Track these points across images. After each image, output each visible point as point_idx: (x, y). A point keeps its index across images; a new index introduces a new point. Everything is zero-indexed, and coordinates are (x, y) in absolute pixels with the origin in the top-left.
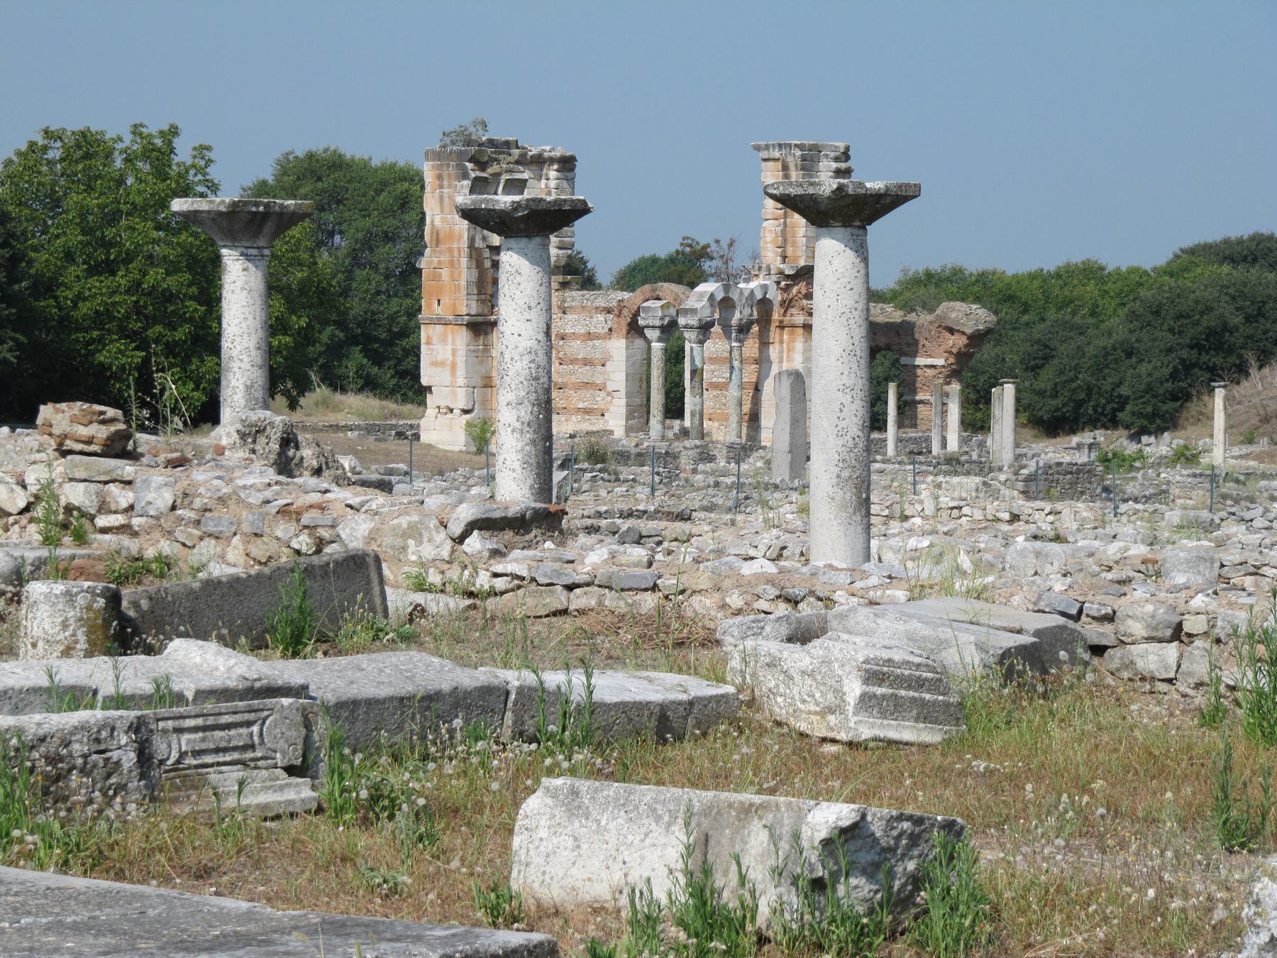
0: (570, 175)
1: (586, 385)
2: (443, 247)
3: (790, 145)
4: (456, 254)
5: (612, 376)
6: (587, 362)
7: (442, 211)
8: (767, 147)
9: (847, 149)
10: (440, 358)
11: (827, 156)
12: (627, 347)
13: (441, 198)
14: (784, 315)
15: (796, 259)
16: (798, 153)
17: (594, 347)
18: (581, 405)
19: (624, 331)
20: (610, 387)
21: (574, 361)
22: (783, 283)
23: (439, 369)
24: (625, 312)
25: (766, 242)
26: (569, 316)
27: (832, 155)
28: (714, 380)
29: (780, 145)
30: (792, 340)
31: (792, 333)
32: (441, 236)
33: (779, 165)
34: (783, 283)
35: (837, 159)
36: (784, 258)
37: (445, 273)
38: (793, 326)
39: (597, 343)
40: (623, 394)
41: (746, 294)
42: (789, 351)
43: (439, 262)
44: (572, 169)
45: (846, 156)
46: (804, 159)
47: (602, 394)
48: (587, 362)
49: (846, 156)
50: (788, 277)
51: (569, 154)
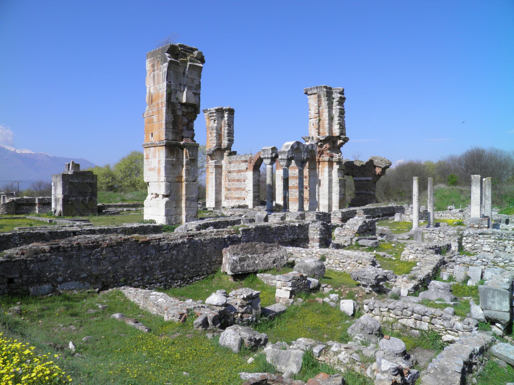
0: (232, 116)
1: (238, 189)
2: (154, 103)
3: (321, 87)
4: (160, 106)
6: (238, 180)
7: (154, 84)
8: (311, 89)
9: (343, 90)
10: (152, 166)
11: (336, 92)
12: (253, 175)
13: (154, 76)
14: (320, 157)
15: (324, 133)
16: (325, 90)
18: (236, 196)
19: (252, 169)
20: (247, 189)
21: (234, 180)
22: (319, 144)
23: (152, 172)
24: (252, 161)
25: (311, 128)
26: (232, 165)
27: (338, 91)
29: (317, 88)
30: (323, 167)
31: (323, 164)
32: (154, 97)
33: (317, 95)
34: (319, 144)
35: (340, 93)
36: (319, 133)
37: (155, 118)
38: (324, 161)
39: (242, 173)
41: (306, 147)
42: (322, 172)
43: (152, 113)
44: (233, 114)
45: (342, 93)
46: (327, 92)
47: (244, 192)
48: (238, 180)
49: (342, 93)
50: (321, 141)
51: (232, 108)
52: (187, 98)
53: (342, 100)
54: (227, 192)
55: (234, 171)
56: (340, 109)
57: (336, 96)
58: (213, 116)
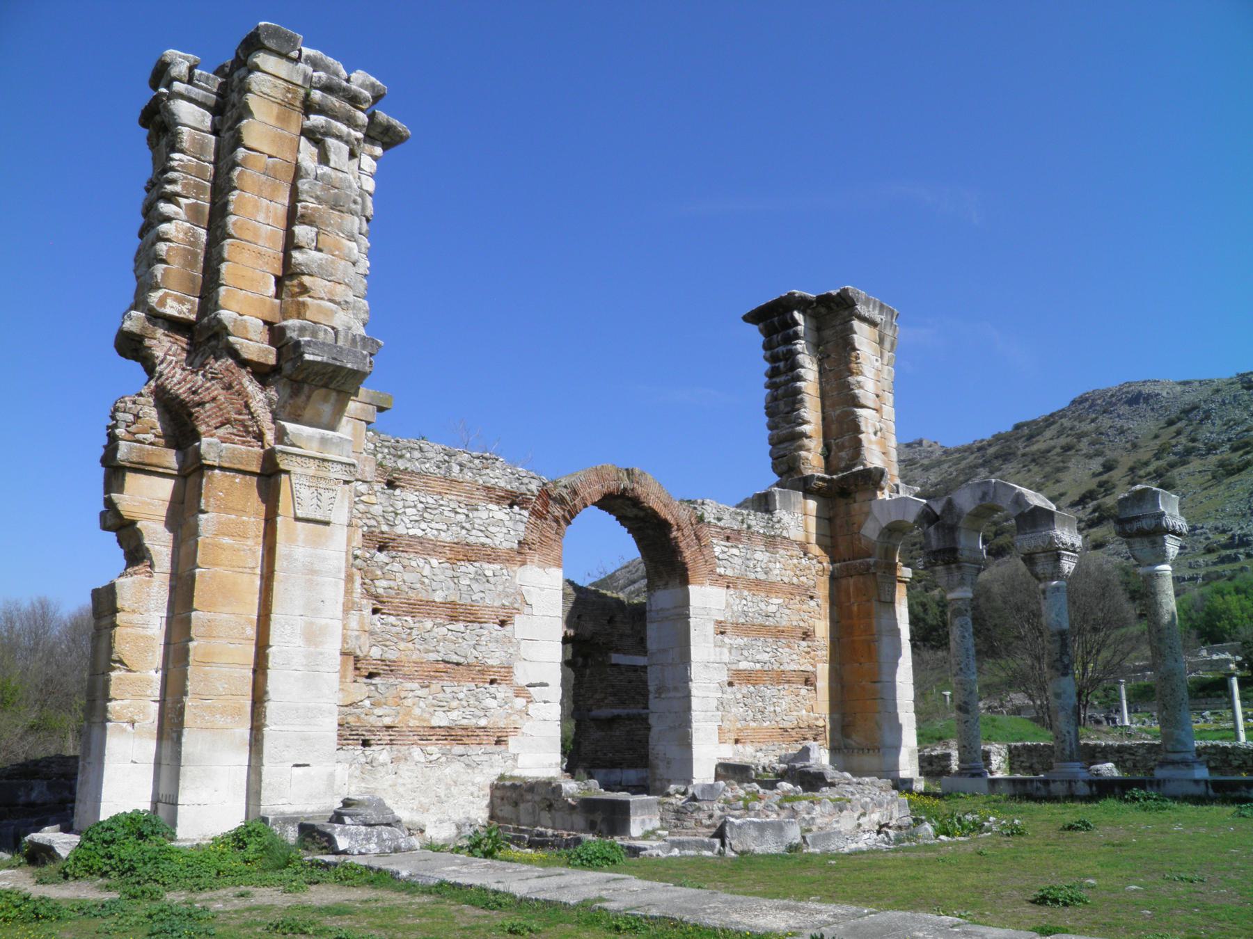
1: (452, 668)
5: (527, 650)
17: (480, 577)
18: (440, 719)
20: (522, 676)
21: (416, 608)
25: (870, 442)
28: (744, 665)
39: (489, 568)
40: (555, 692)
47: (502, 691)
54: (361, 690)
55: (426, 547)
58: (350, 122)
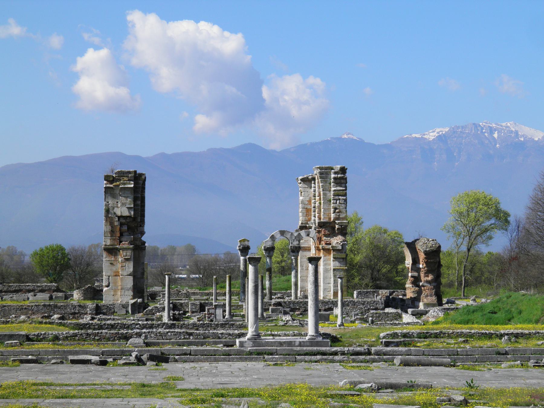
35: (335, 173)
45: (343, 170)
49: (343, 170)
52: (121, 213)
53: (338, 181)
56: (334, 191)
57: (333, 176)
